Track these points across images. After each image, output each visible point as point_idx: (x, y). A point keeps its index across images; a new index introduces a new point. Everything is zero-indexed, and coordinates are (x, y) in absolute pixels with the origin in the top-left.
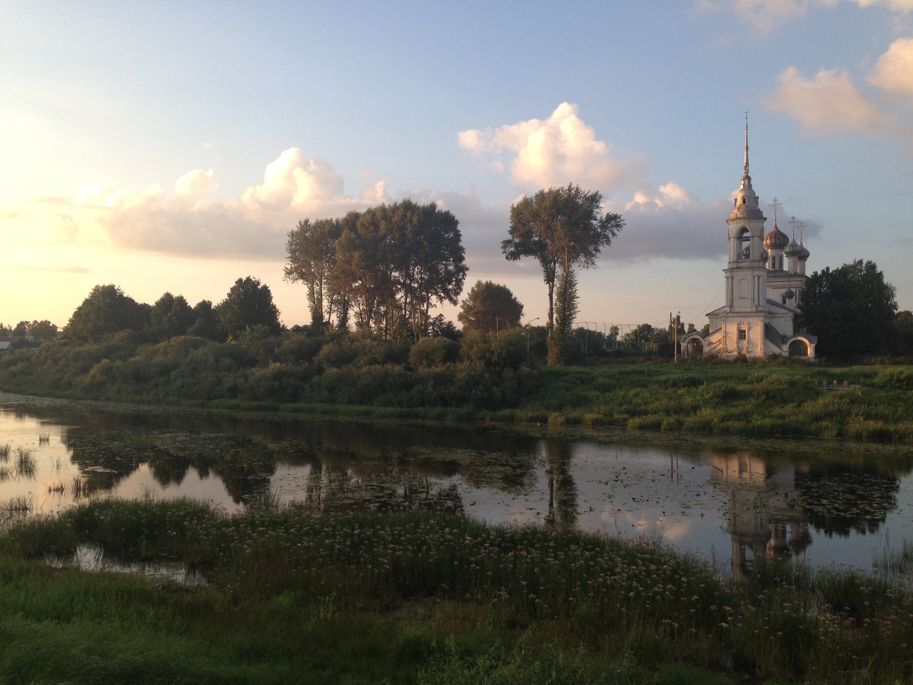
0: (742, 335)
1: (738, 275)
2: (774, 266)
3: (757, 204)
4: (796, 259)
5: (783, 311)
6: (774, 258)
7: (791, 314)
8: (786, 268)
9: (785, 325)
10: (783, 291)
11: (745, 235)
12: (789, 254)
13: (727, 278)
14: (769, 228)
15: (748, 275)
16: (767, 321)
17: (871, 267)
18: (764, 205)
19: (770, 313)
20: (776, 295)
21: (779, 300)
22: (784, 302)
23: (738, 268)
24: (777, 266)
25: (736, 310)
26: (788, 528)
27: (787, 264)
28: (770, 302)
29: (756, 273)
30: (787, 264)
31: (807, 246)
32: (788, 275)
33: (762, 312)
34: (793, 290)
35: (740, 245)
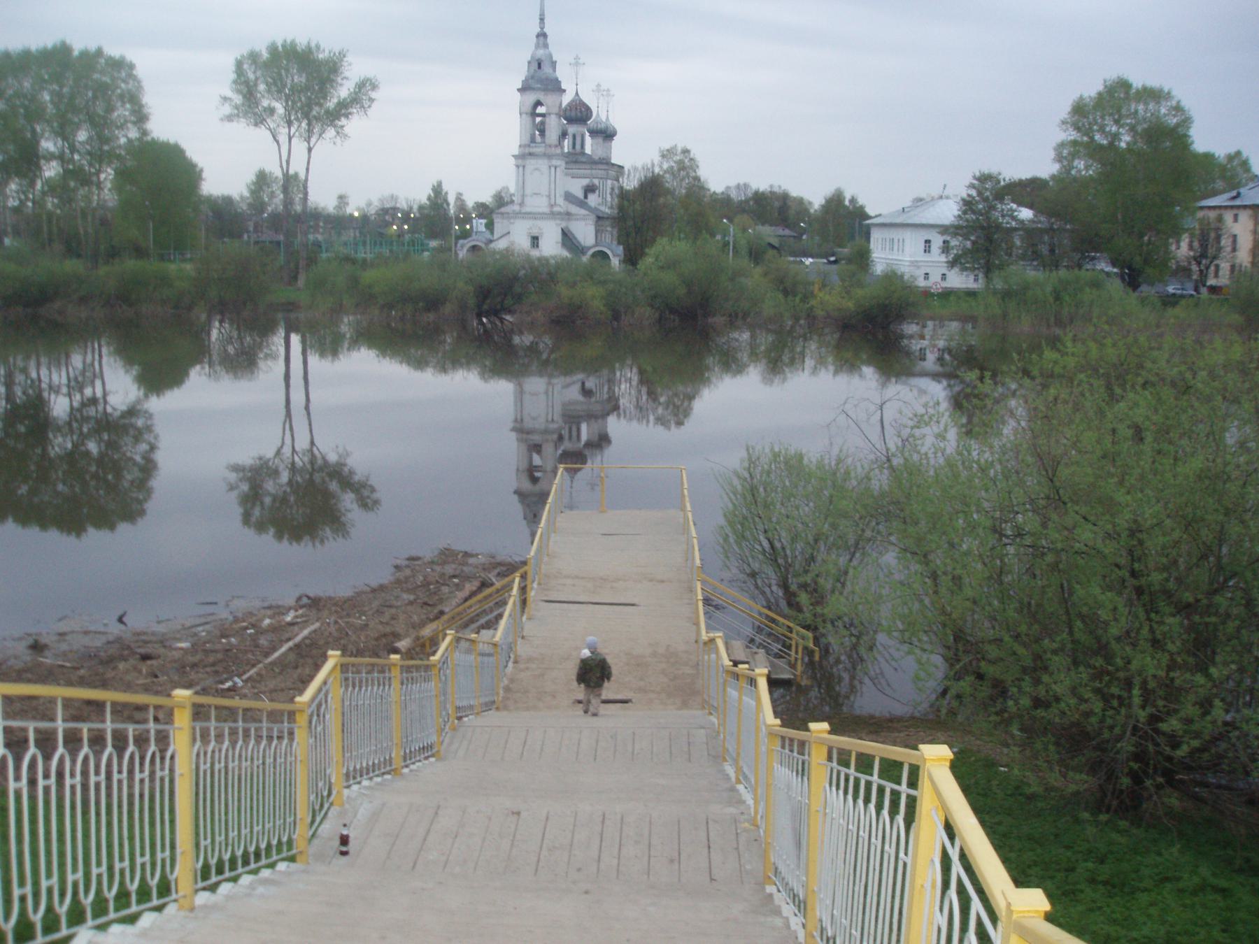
0: (535, 240)
1: (531, 163)
2: (574, 147)
3: (554, 70)
4: (600, 140)
5: (583, 212)
6: (574, 137)
7: (593, 217)
8: (588, 150)
9: (585, 233)
10: (585, 182)
11: (540, 110)
12: (594, 133)
13: (518, 166)
14: (566, 99)
15: (543, 164)
16: (564, 224)
17: (686, 151)
18: (563, 74)
19: (568, 214)
20: (577, 187)
21: (579, 194)
22: (586, 197)
23: (530, 154)
24: (578, 147)
25: (528, 209)
26: (584, 427)
27: (590, 146)
28: (569, 197)
29: (554, 162)
30: (589, 145)
31: (617, 121)
32: (593, 162)
33: (559, 213)
34: (596, 181)
35: (534, 121)
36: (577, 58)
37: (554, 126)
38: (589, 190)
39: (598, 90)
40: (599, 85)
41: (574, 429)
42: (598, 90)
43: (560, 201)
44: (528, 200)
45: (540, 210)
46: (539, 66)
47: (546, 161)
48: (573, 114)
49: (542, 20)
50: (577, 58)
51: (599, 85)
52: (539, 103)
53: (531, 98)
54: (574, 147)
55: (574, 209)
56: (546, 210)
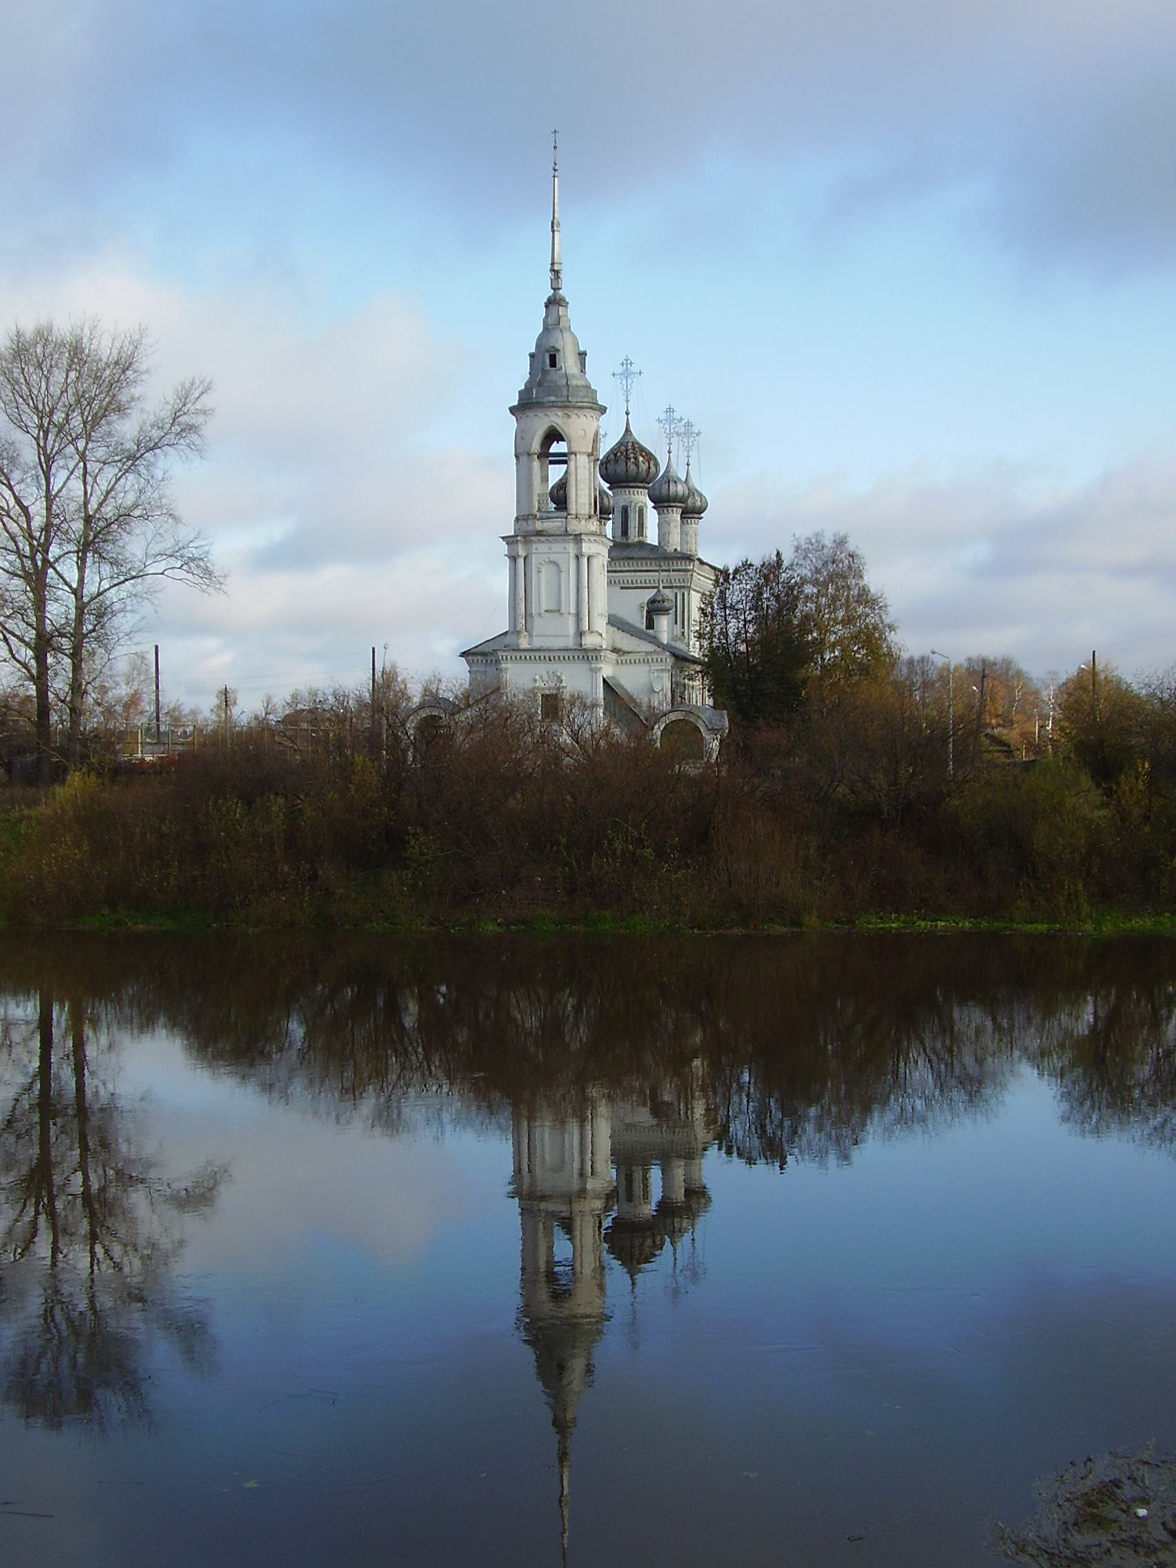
1: (541, 550)
11: (556, 448)
12: (661, 502)
22: (650, 625)
26: (655, 1174)
31: (707, 484)
32: (659, 556)
36: (627, 363)
37: (586, 485)
38: (655, 609)
39: (670, 421)
40: (670, 410)
41: (638, 1175)
42: (670, 421)
43: (601, 624)
44: (539, 625)
45: (559, 643)
46: (553, 363)
47: (571, 548)
48: (621, 468)
49: (556, 273)
50: (627, 363)
51: (670, 410)
52: (554, 435)
53: (540, 424)
54: (625, 532)
55: (626, 642)
56: (570, 643)
